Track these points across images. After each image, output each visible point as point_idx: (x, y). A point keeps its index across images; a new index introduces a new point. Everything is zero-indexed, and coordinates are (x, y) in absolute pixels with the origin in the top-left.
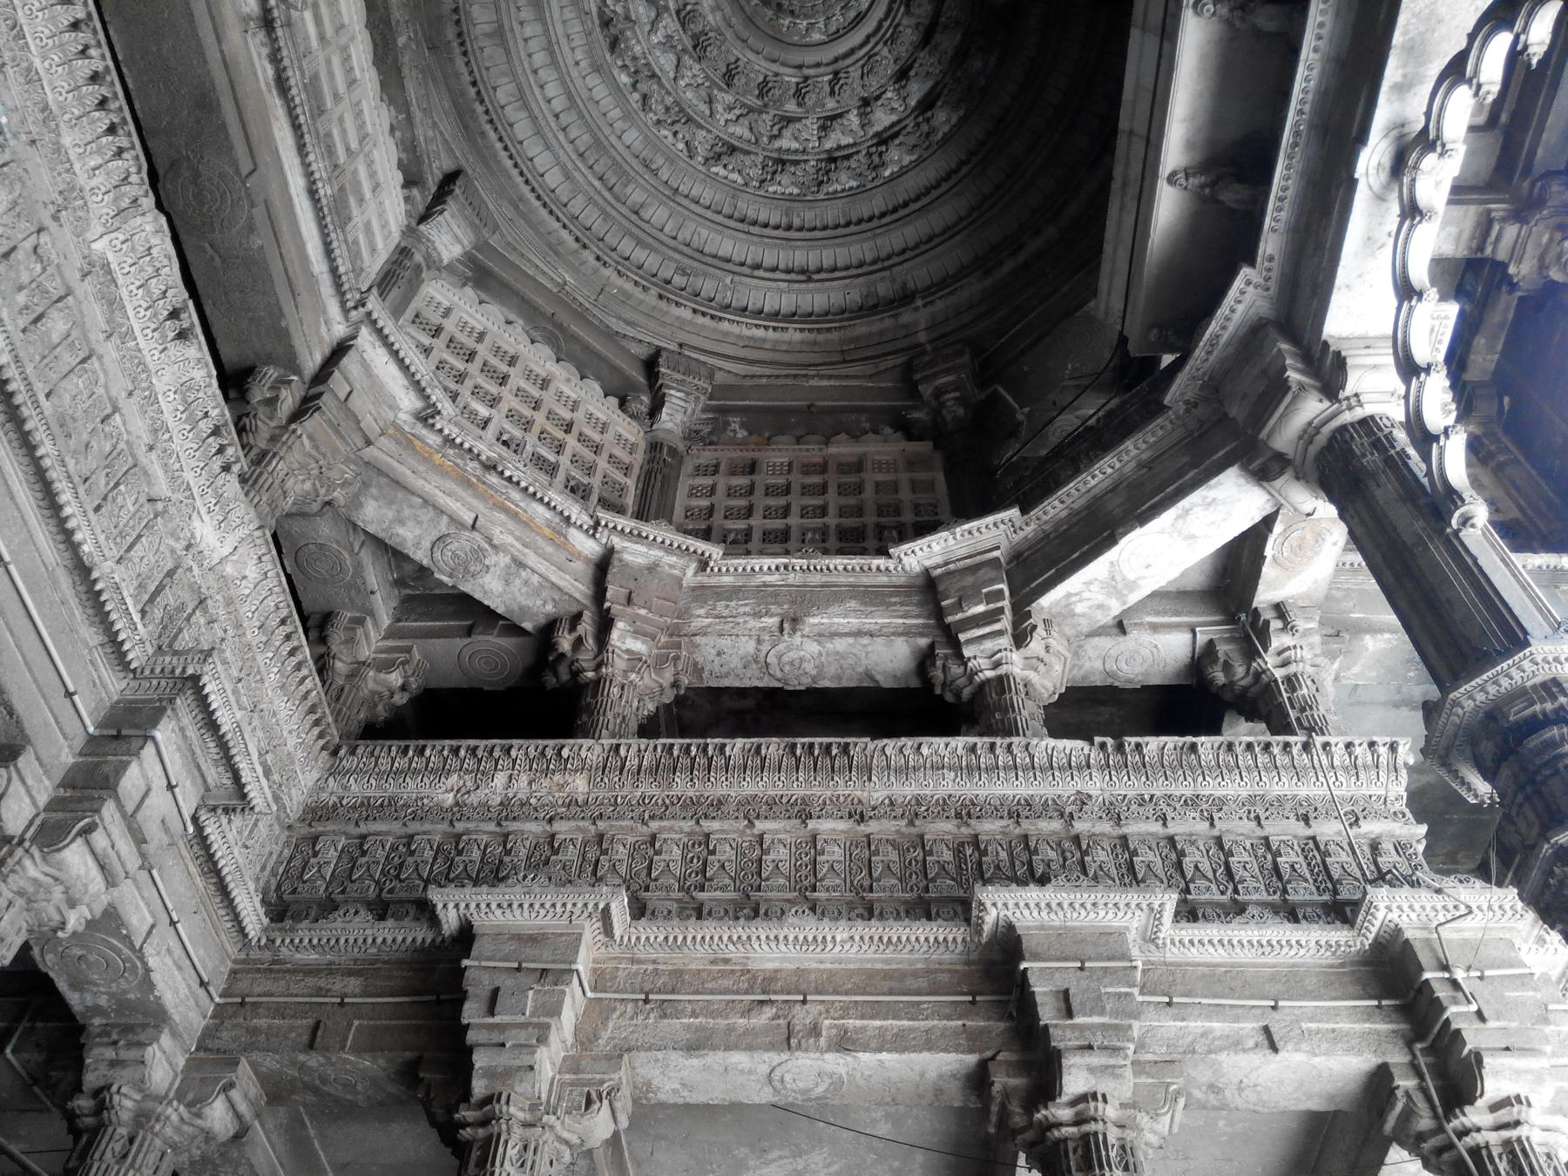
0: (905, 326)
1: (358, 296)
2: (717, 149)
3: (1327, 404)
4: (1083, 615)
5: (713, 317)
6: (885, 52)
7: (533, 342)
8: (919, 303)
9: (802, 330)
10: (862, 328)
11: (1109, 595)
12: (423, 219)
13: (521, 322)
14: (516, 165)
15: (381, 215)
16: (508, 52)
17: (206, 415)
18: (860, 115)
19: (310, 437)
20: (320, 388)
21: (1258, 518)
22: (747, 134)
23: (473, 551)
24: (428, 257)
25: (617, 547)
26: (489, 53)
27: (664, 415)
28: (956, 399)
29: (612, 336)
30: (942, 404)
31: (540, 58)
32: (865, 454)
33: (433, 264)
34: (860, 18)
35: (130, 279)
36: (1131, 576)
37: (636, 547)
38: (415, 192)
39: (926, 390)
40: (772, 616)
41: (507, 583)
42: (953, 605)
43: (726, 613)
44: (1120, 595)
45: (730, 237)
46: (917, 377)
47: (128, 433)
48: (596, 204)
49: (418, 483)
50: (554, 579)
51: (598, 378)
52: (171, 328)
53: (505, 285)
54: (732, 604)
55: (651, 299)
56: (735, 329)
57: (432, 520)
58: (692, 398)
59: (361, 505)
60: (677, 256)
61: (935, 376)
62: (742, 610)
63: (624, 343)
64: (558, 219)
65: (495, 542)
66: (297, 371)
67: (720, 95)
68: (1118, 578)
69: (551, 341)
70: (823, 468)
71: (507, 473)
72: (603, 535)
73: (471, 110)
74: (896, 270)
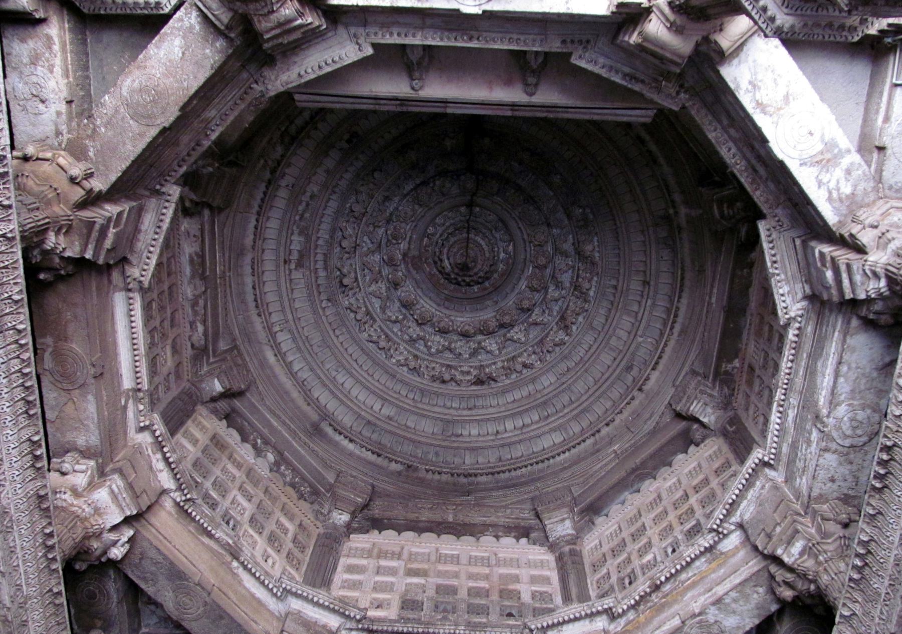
3: (653, 16)
7: (639, 491)
11: (837, 165)
12: (547, 537)
13: (626, 493)
14: (548, 459)
15: (529, 564)
16: (483, 448)
24: (569, 543)
25: (739, 520)
27: (705, 420)
29: (653, 433)
33: (575, 540)
37: (742, 507)
38: (532, 535)
41: (734, 612)
45: (615, 330)
50: (737, 581)
51: (675, 453)
53: (600, 498)
54: (799, 454)
58: (699, 395)
60: (618, 371)
63: (661, 425)
65: (697, 611)
67: (534, 317)
69: (642, 478)
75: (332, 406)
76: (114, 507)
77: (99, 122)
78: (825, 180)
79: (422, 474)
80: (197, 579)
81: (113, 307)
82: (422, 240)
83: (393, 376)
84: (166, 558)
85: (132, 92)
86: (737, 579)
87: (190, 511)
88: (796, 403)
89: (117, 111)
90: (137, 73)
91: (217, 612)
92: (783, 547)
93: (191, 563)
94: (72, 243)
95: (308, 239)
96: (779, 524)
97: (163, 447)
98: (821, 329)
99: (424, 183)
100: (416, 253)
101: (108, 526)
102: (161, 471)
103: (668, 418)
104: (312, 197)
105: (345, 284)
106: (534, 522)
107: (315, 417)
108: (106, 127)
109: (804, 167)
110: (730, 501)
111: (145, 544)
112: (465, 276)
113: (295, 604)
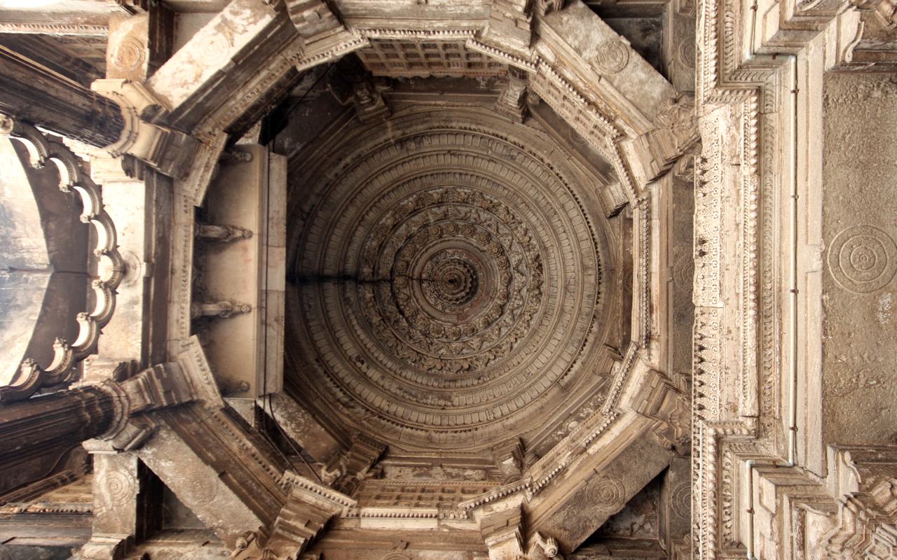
0: (399, 129)
1: (641, 206)
2: (494, 210)
4: (245, 8)
5: (497, 136)
6: (418, 246)
8: (392, 141)
9: (452, 127)
10: (421, 128)
16: (582, 262)
17: (705, 195)
18: (428, 220)
19: (673, 146)
20: (664, 169)
21: (157, 73)
22: (481, 213)
23: (603, 61)
25: (527, 49)
26: (590, 263)
27: (518, 94)
28: (363, 100)
30: (370, 97)
31: (569, 256)
32: (409, 70)
34: (431, 258)
35: (714, 282)
36: (221, 35)
37: (517, 49)
38: (628, 216)
39: (380, 102)
40: (434, 6)
42: (324, 13)
43: (462, 7)
44: (225, 21)
46: (386, 109)
47: (735, 210)
48: (551, 192)
49: (627, 104)
50: (560, 39)
52: (705, 248)
54: (459, 12)
55: (528, 147)
56: (486, 129)
57: (624, 83)
58: (504, 102)
59: (662, 94)
61: (376, 110)
62: (453, 9)
64: (569, 188)
66: (675, 178)
68: (228, 34)
70: (430, 64)
71: (582, 100)
72: (535, 58)
73: (602, 242)
74: (406, 155)
75: (551, 376)
76: (505, 546)
77: (215, 524)
78: (243, 28)
79: (600, 307)
80: (583, 483)
81: (370, 530)
82: (446, 314)
83: (535, 332)
84: (563, 508)
85: (195, 498)
86: (560, 39)
87: (541, 485)
88: (428, 22)
89: (208, 510)
90: (182, 494)
91: (615, 467)
92: (515, 7)
93: (574, 487)
94: (286, 551)
95: (431, 392)
96: (504, 16)
97: (484, 502)
98: (363, 15)
99: (402, 312)
100: (455, 317)
101: (520, 553)
102: (507, 506)
103: (531, 121)
104: (400, 389)
105: (467, 367)
106: (621, 216)
107: (556, 390)
108: (219, 519)
109: (235, 44)
110: (510, 58)
111: (550, 524)
112: (465, 282)
113: (625, 402)
